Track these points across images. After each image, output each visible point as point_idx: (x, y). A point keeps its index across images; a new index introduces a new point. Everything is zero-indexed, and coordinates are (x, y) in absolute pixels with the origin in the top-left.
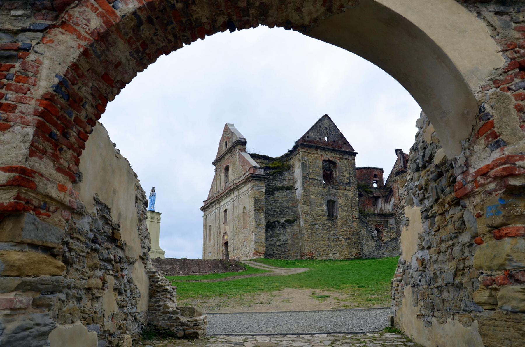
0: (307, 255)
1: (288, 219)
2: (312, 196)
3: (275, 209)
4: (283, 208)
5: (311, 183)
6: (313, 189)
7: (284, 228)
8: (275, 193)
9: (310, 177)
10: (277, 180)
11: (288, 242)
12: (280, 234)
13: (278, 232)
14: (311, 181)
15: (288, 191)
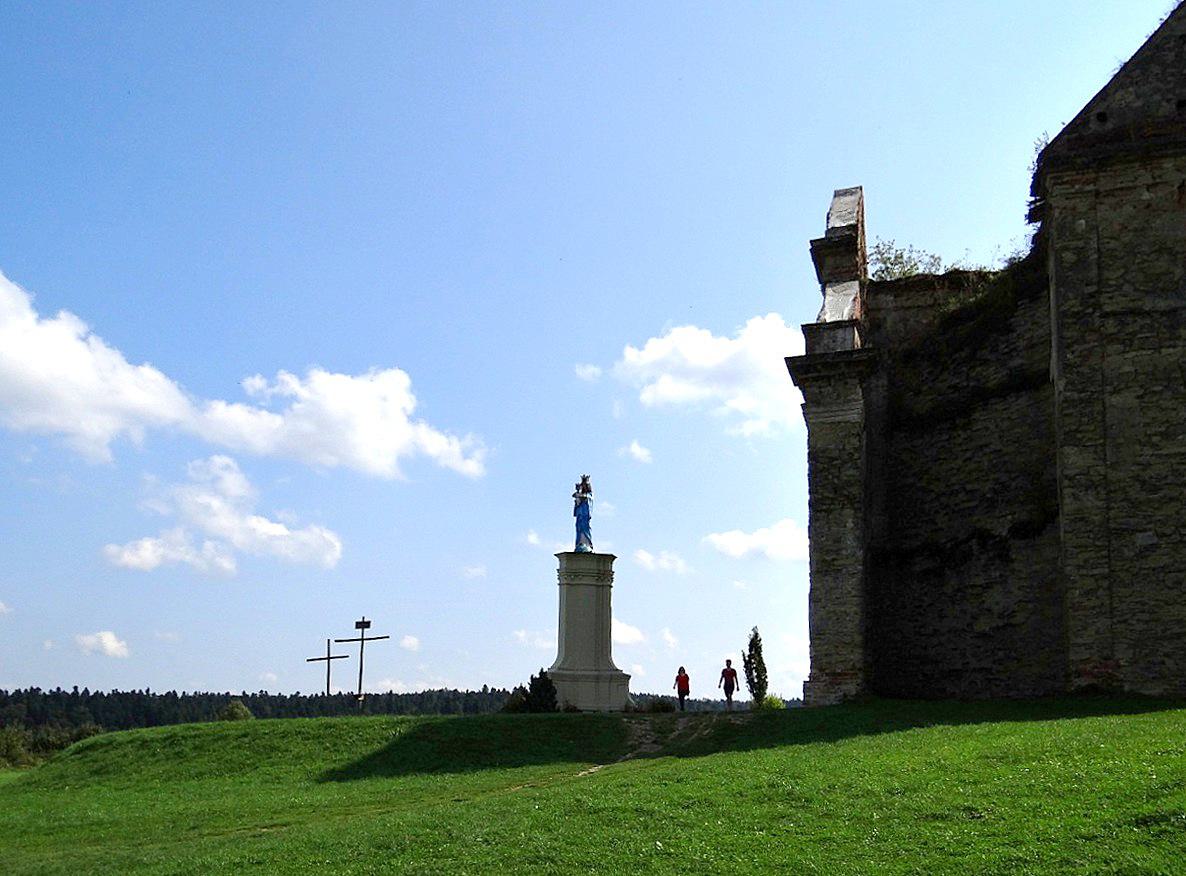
0: (1079, 674)
1: (1024, 516)
2: (1115, 400)
3: (976, 486)
4: (1004, 478)
5: (1111, 339)
6: (1120, 361)
7: (1004, 557)
8: (977, 415)
9: (1108, 309)
10: (985, 362)
11: (1019, 618)
12: (988, 587)
13: (980, 581)
14: (1111, 326)
15: (1023, 401)
